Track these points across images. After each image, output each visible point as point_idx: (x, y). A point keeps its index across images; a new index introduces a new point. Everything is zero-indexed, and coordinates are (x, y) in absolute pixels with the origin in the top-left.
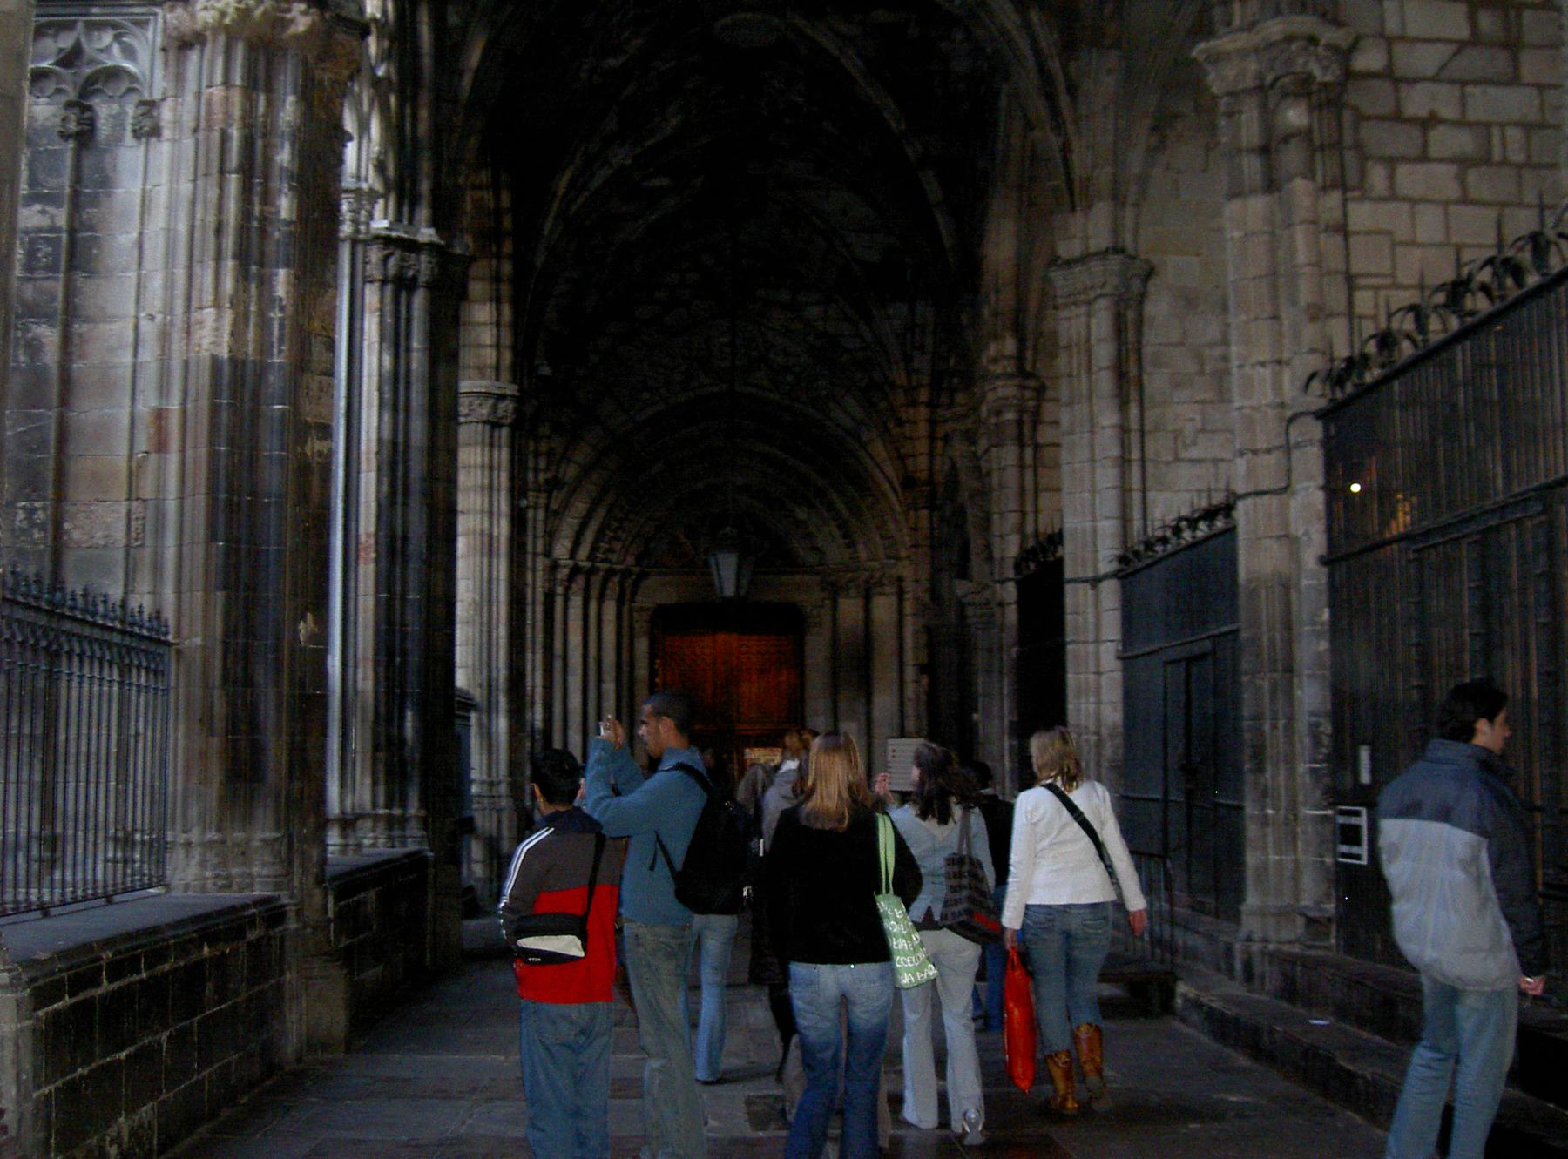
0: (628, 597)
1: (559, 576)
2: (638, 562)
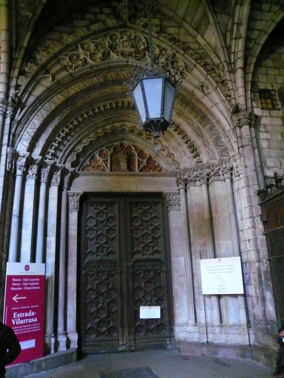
0: (66, 186)
1: (19, 163)
2: (73, 165)
